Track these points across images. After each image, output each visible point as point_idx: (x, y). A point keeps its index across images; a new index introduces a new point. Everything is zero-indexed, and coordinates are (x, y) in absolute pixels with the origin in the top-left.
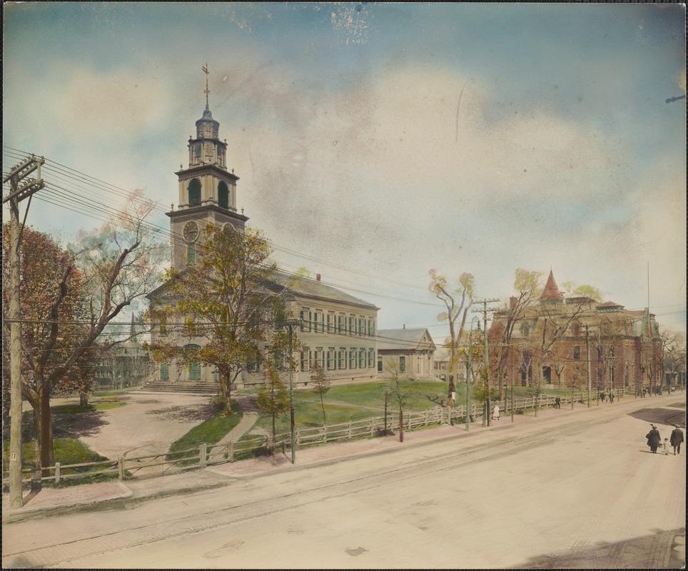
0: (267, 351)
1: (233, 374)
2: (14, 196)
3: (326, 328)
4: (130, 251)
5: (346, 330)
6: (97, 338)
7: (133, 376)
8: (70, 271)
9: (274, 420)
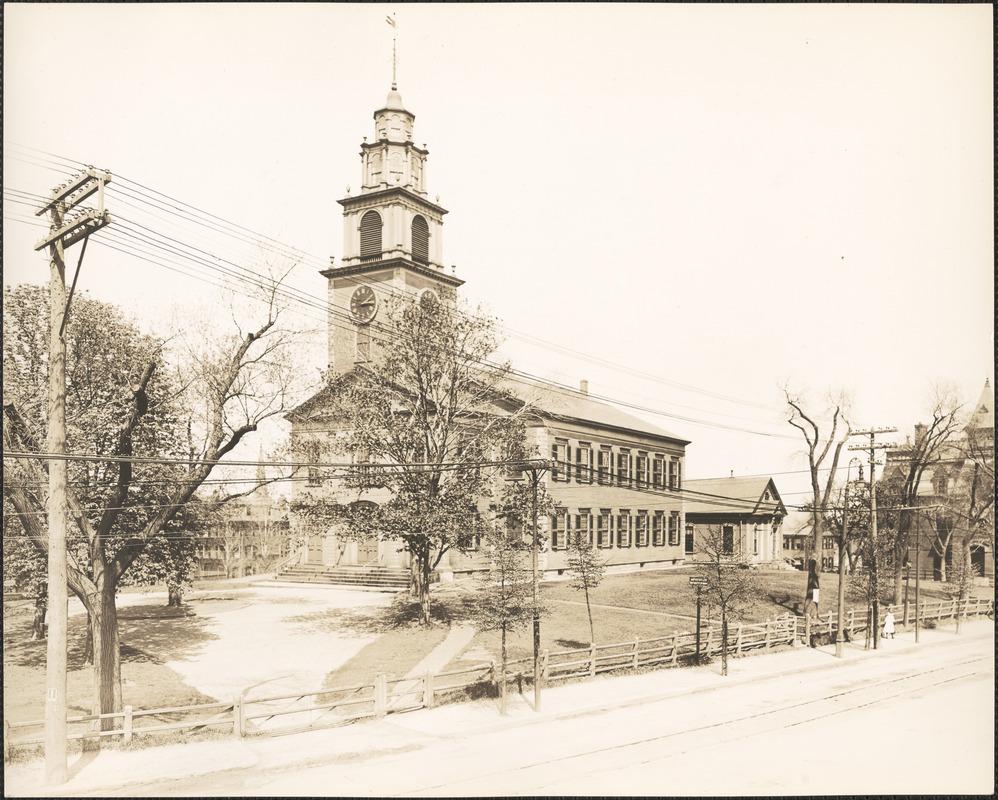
0: (493, 514)
1: (434, 553)
2: (57, 239)
3: (596, 475)
4: (258, 337)
5: (631, 480)
6: (200, 488)
7: (260, 556)
9: (504, 635)
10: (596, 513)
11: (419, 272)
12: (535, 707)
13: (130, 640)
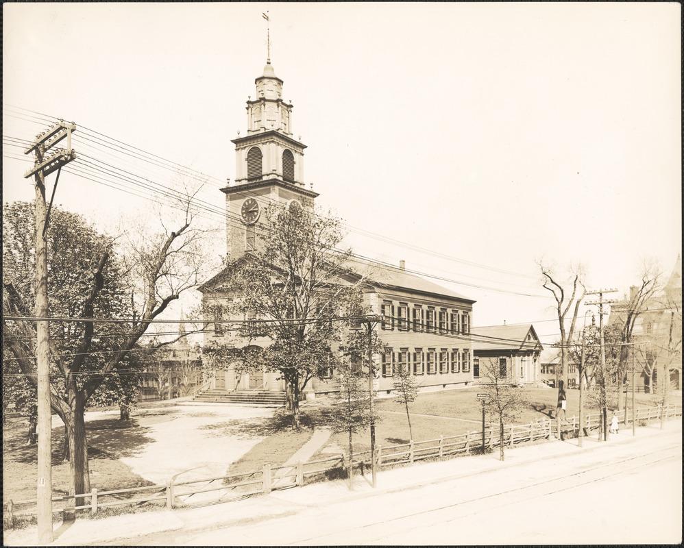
0: (342, 353)
1: (301, 381)
2: (39, 170)
3: (411, 325)
4: (179, 234)
5: (436, 328)
6: (140, 339)
7: (183, 384)
8: (106, 259)
10: (412, 351)
12: (373, 485)
13: (94, 443)
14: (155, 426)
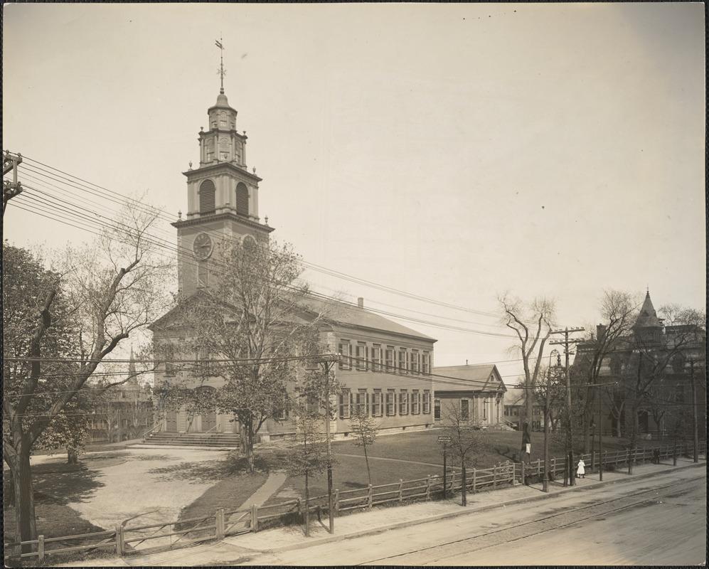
0: (297, 394)
1: (256, 422)
3: (370, 365)
5: (395, 368)
7: (133, 426)
8: (54, 295)
10: (370, 392)
11: (243, 223)
12: (330, 530)
13: (41, 488)
14: (104, 470)
